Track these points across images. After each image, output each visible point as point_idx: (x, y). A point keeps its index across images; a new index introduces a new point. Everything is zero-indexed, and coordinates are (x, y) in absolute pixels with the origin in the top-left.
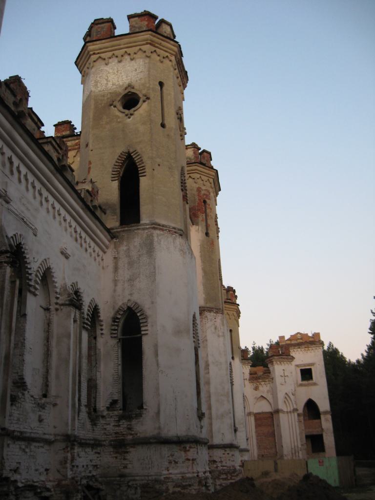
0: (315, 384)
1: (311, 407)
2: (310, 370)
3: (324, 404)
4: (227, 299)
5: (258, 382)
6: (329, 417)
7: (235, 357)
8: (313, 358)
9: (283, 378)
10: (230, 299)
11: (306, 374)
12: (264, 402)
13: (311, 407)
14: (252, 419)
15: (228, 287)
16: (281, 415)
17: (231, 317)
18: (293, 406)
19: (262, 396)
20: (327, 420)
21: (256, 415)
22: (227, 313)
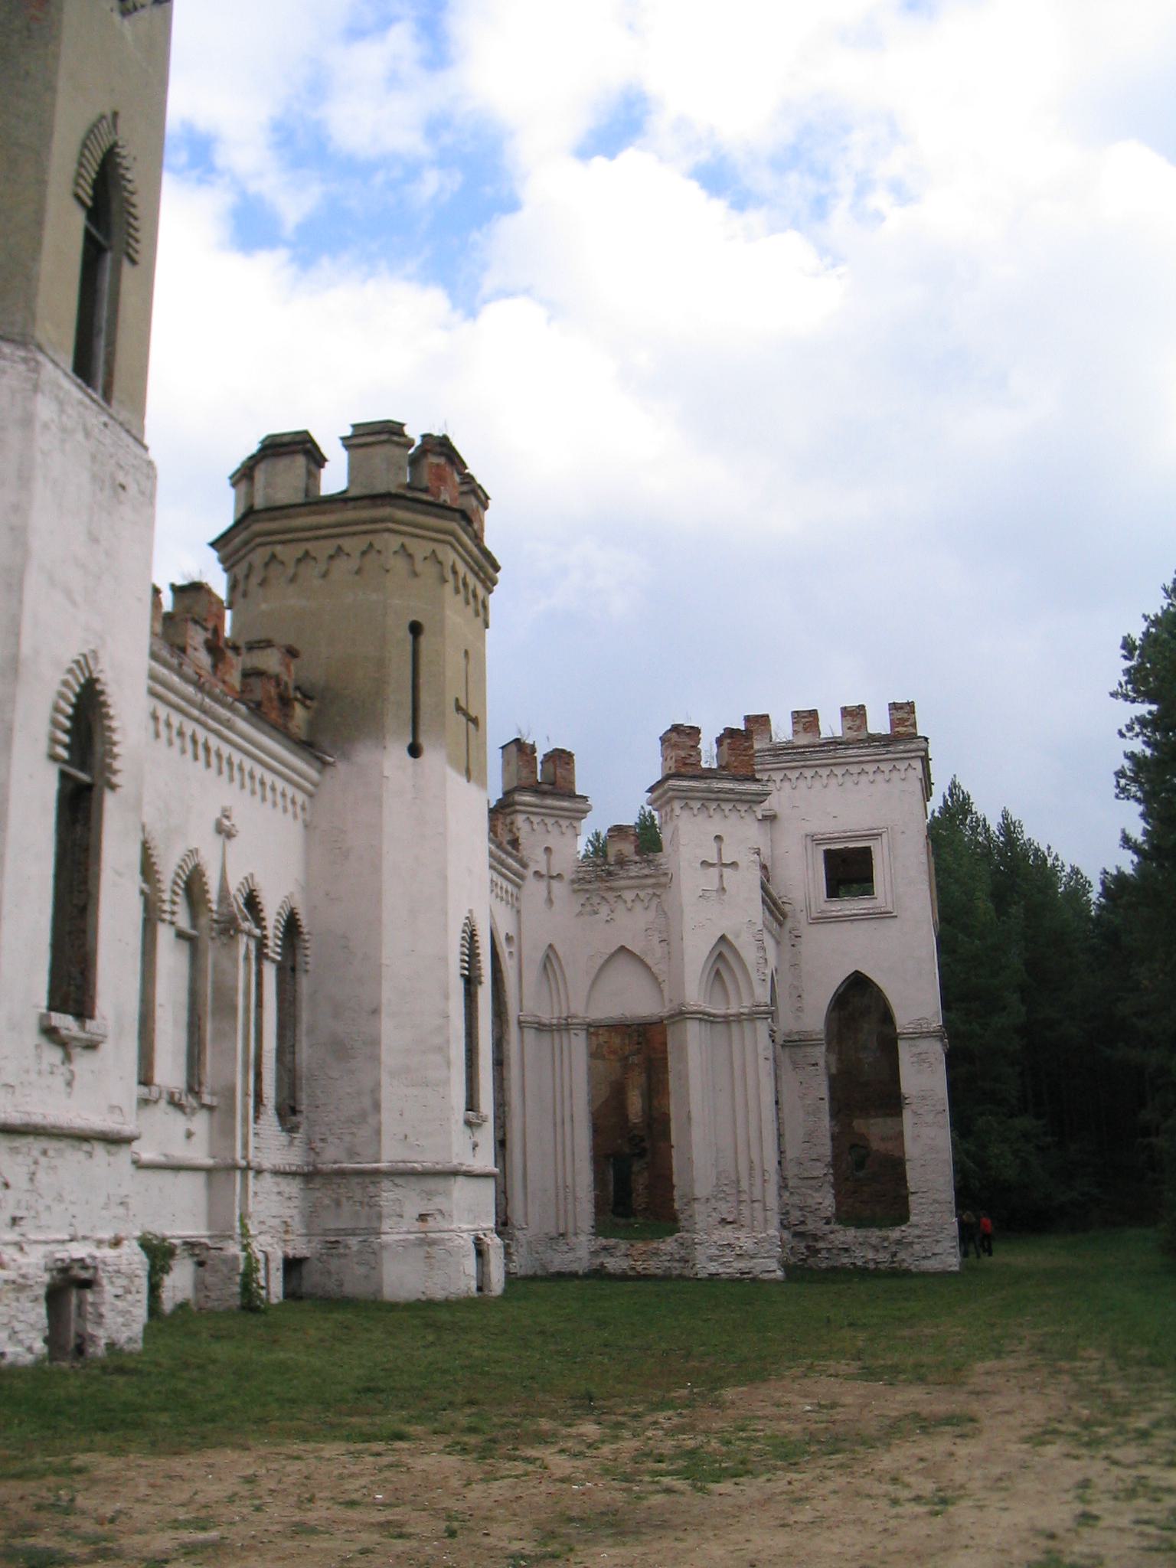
0: (885, 915)
1: (858, 998)
2: (867, 851)
3: (916, 997)
4: (409, 487)
5: (610, 889)
6: (936, 1051)
7: (423, 741)
8: (883, 812)
9: (714, 872)
10: (426, 490)
11: (849, 870)
12: (625, 976)
13: (858, 998)
14: (578, 1045)
15: (425, 437)
16: (693, 1030)
17: (420, 566)
18: (752, 995)
19: (623, 948)
20: (920, 1058)
21: (593, 1029)
22: (403, 546)
